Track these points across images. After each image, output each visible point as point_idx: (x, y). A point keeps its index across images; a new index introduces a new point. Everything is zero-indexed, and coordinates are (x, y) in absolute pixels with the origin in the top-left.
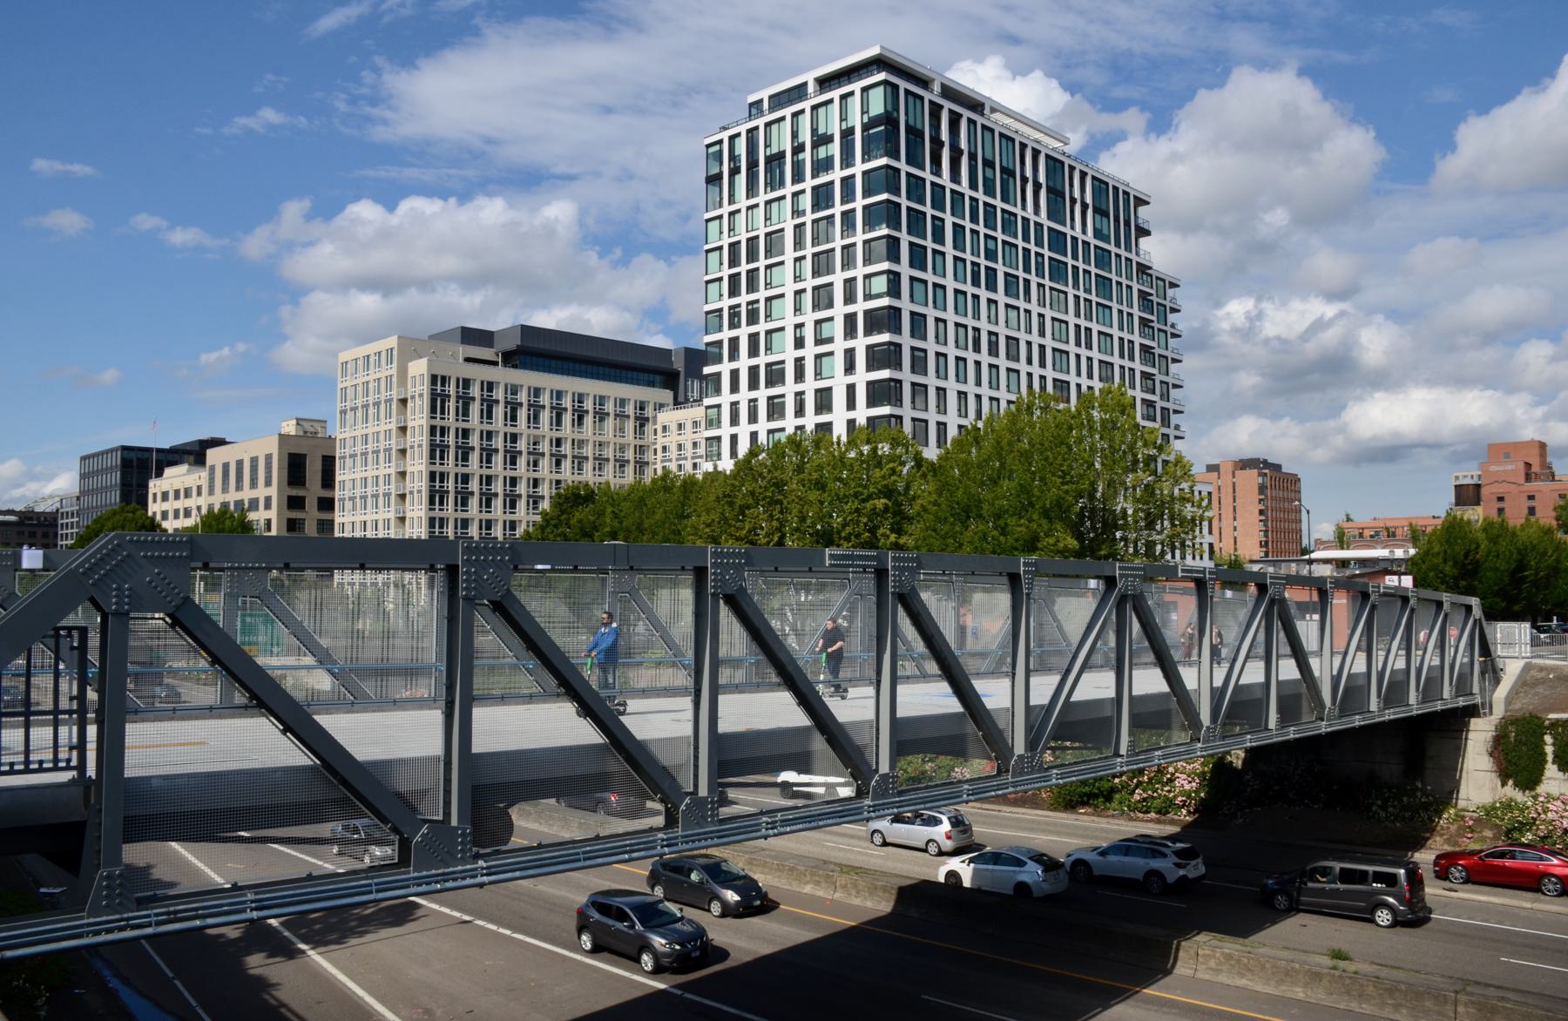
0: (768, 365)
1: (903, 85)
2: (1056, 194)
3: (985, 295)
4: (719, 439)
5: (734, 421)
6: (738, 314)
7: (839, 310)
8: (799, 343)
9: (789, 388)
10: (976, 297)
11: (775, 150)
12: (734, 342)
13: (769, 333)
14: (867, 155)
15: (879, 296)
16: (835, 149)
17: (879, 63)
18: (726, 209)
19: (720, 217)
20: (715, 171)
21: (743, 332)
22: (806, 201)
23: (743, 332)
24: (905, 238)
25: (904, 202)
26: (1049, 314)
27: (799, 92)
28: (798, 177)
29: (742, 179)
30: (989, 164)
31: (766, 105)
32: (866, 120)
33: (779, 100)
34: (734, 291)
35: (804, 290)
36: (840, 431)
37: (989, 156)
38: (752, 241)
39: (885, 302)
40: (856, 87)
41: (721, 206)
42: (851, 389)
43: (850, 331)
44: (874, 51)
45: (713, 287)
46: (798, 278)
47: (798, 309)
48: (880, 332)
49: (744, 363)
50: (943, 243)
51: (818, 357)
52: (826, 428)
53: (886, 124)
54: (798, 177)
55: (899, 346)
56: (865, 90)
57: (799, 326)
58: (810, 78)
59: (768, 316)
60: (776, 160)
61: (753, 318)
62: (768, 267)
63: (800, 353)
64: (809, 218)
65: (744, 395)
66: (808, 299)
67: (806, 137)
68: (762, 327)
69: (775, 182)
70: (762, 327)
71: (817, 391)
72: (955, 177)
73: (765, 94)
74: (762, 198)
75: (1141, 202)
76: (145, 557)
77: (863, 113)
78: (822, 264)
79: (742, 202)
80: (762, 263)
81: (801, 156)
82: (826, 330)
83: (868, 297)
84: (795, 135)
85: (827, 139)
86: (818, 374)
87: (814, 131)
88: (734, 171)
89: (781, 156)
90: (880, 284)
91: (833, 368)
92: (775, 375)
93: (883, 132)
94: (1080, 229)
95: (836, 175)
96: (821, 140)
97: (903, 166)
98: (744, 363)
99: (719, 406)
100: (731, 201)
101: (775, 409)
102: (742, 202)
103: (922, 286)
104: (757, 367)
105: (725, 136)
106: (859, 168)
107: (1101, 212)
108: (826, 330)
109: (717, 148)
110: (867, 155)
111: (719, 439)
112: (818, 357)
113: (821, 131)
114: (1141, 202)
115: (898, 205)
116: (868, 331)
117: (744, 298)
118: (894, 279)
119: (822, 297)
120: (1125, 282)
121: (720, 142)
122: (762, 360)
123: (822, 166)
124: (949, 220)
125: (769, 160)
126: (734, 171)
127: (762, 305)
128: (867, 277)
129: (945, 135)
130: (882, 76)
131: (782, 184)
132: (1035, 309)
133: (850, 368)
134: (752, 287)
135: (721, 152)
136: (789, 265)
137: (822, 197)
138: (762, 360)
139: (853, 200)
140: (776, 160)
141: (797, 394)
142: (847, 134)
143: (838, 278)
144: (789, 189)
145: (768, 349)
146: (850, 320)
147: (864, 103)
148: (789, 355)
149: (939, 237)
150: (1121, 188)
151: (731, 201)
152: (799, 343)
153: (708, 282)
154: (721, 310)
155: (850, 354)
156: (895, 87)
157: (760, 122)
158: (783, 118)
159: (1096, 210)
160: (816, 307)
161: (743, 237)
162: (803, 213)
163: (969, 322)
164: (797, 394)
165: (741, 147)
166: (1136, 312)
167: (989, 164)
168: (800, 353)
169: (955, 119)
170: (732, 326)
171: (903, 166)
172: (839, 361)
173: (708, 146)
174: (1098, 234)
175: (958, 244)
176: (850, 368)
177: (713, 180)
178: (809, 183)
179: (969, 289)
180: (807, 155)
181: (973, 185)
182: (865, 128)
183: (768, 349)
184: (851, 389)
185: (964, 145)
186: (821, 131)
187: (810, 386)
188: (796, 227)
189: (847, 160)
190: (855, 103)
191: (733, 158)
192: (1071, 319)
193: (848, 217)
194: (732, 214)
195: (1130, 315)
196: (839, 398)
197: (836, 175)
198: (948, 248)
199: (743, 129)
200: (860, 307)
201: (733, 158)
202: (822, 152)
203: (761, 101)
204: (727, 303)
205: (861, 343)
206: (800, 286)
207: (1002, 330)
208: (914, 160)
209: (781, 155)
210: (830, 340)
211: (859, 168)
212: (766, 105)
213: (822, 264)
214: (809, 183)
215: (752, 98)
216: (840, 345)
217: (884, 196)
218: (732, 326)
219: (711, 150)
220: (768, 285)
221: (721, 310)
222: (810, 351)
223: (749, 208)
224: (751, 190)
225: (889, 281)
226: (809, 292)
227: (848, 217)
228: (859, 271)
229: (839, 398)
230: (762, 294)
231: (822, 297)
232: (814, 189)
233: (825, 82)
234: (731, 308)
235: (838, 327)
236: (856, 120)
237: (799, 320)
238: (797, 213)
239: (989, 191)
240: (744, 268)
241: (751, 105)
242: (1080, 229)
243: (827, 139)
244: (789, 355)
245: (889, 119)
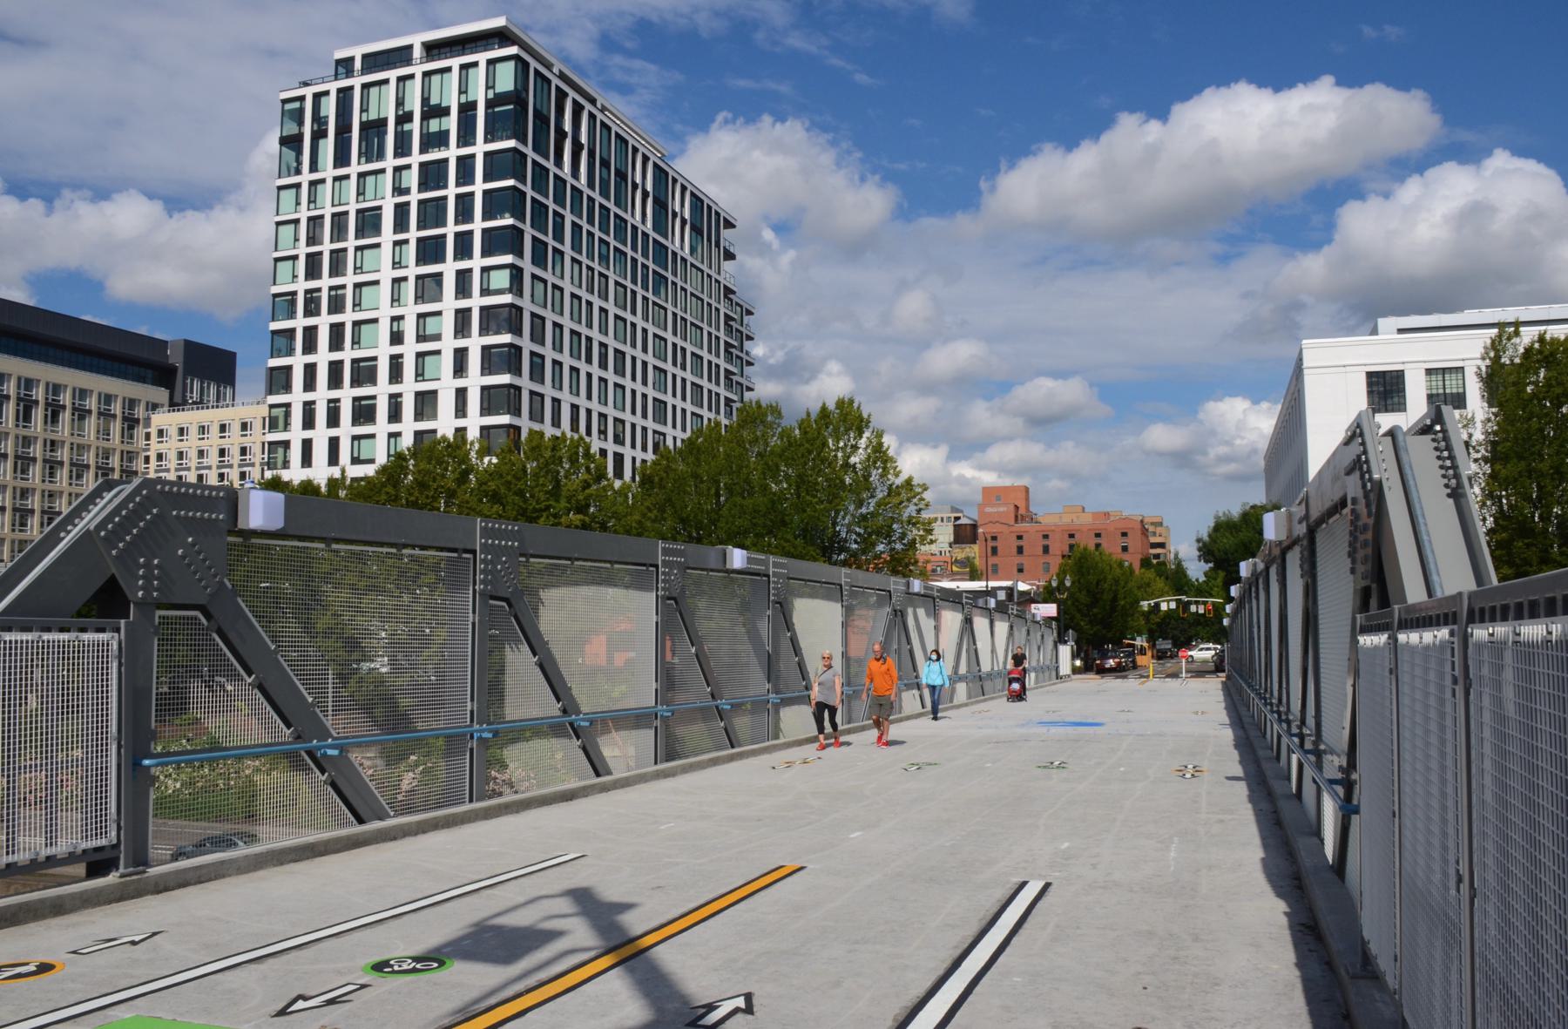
0: (354, 361)
1: (533, 64)
2: (661, 205)
3: (598, 304)
4: (286, 445)
5: (309, 423)
6: (318, 301)
7: (449, 303)
8: (397, 338)
9: (382, 390)
10: (589, 304)
11: (373, 115)
12: (311, 332)
13: (357, 324)
14: (490, 136)
15: (499, 292)
16: (452, 123)
17: (501, 37)
18: (306, 177)
19: (298, 186)
20: (291, 129)
21: (324, 322)
22: (412, 179)
23: (324, 322)
24: (529, 232)
25: (530, 193)
26: (652, 329)
27: (401, 56)
28: (402, 148)
29: (328, 146)
30: (605, 164)
31: (358, 65)
32: (491, 95)
33: (375, 61)
34: (313, 270)
35: (405, 279)
36: (473, 434)
37: (605, 156)
38: (339, 219)
39: (507, 299)
40: (482, 57)
41: (298, 172)
42: (461, 394)
43: (462, 327)
44: (499, 22)
45: (284, 267)
46: (397, 264)
47: (395, 300)
48: (497, 333)
49: (323, 357)
50: (562, 242)
51: (420, 356)
52: (461, 431)
53: (516, 104)
54: (402, 148)
55: (519, 349)
56: (491, 62)
57: (397, 319)
58: (417, 40)
59: (357, 305)
60: (374, 129)
61: (336, 305)
62: (358, 249)
63: (397, 350)
64: (414, 198)
65: (322, 394)
66: (409, 289)
67: (415, 105)
68: (348, 317)
69: (372, 150)
70: (348, 317)
71: (483, 388)
72: (575, 172)
73: (357, 52)
74: (354, 169)
75: (729, 225)
76: (178, 517)
77: (488, 88)
78: (430, 251)
79: (328, 171)
80: (351, 243)
81: (407, 127)
82: (431, 326)
83: (485, 292)
84: (400, 103)
85: (443, 112)
86: (420, 375)
87: (425, 101)
88: (319, 134)
89: (382, 123)
90: (501, 279)
91: (438, 368)
92: (364, 373)
93: (509, 113)
94: (679, 242)
95: (452, 152)
96: (433, 111)
97: (528, 151)
98: (323, 357)
99: (288, 405)
100: (314, 167)
101: (364, 412)
102: (328, 171)
103: (541, 286)
104: (341, 362)
105: (308, 92)
106: (480, 148)
107: (697, 230)
108: (431, 326)
109: (297, 105)
110: (490, 136)
111: (286, 445)
112: (420, 356)
113: (434, 101)
114: (729, 225)
115: (524, 194)
116: (484, 331)
117: (325, 282)
118: (516, 273)
119: (428, 287)
120: (714, 304)
121: (302, 99)
122: (347, 355)
123: (435, 140)
124: (569, 218)
125: (365, 126)
126: (319, 134)
127: (349, 292)
128: (485, 270)
129: (568, 127)
130: (513, 50)
131: (381, 156)
132: (640, 324)
133: (460, 368)
134: (337, 268)
135: (301, 111)
136: (387, 249)
137: (432, 175)
138: (347, 355)
139: (472, 182)
140: (374, 129)
141: (392, 396)
142: (467, 109)
143: (449, 268)
144: (390, 162)
145: (356, 342)
146: (463, 316)
147: (484, 79)
148: (383, 352)
149: (558, 236)
150: (714, 207)
151: (314, 167)
152: (397, 338)
153: (277, 260)
154: (294, 293)
155: (461, 356)
156: (526, 65)
157: (357, 82)
158: (386, 81)
159: (693, 228)
160: (420, 298)
161: (328, 212)
162: (407, 191)
163: (584, 330)
164: (392, 396)
165: (330, 108)
166: (722, 334)
167: (605, 164)
168: (397, 350)
169: (578, 110)
170: (309, 312)
171: (528, 151)
172: (447, 360)
173: (285, 101)
174: (693, 250)
175: (576, 246)
176: (460, 368)
177: (291, 142)
178: (416, 158)
179: (585, 296)
180: (415, 126)
181: (591, 185)
182: (490, 104)
183: (356, 342)
184: (461, 394)
185: (584, 139)
186: (434, 101)
187: (409, 388)
188: (397, 206)
189: (466, 137)
190: (479, 75)
191: (318, 119)
192: (670, 338)
193: (465, 202)
194: (313, 184)
195: (717, 338)
196: (446, 403)
197: (452, 152)
198: (567, 248)
199: (333, 87)
200: (476, 302)
201: (318, 119)
202: (434, 125)
203: (352, 59)
204: (302, 286)
205: (475, 343)
206: (399, 273)
207: (612, 343)
208: (539, 147)
209: (382, 123)
210: (437, 337)
211: (480, 148)
212: (358, 65)
213: (430, 251)
214: (416, 158)
215: (341, 54)
216: (448, 344)
217: (510, 182)
218: (309, 312)
219: (288, 106)
220: (358, 269)
221: (294, 293)
222: (410, 348)
223: (336, 179)
224: (342, 159)
225: (512, 276)
226: (412, 281)
227: (465, 202)
228: (477, 262)
229: (446, 403)
230: (349, 279)
231: (428, 287)
232: (422, 165)
233: (434, 49)
234: (307, 292)
235: (448, 324)
236: (479, 95)
237: (397, 312)
238: (399, 190)
239: (605, 193)
240: (326, 247)
241: (339, 62)
242: (679, 242)
243: (443, 112)
244: (383, 352)
245: (517, 97)
